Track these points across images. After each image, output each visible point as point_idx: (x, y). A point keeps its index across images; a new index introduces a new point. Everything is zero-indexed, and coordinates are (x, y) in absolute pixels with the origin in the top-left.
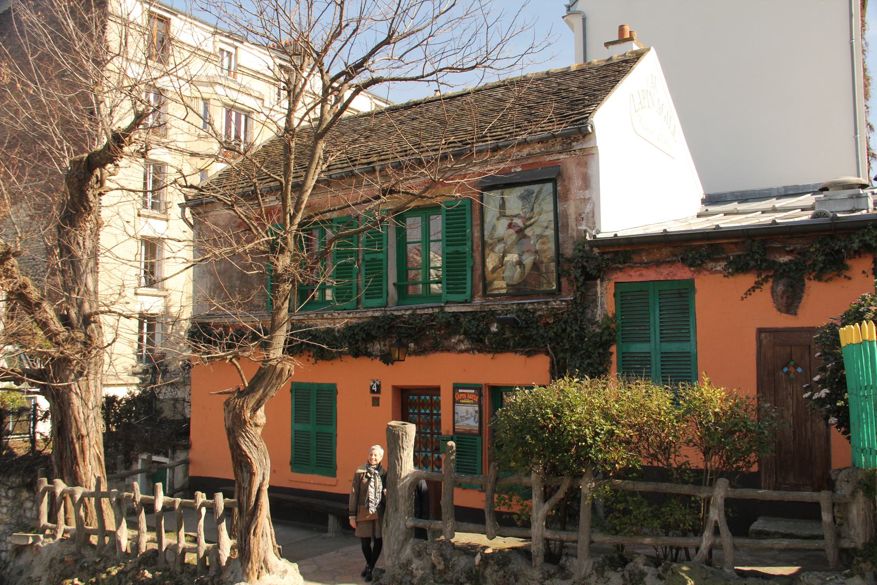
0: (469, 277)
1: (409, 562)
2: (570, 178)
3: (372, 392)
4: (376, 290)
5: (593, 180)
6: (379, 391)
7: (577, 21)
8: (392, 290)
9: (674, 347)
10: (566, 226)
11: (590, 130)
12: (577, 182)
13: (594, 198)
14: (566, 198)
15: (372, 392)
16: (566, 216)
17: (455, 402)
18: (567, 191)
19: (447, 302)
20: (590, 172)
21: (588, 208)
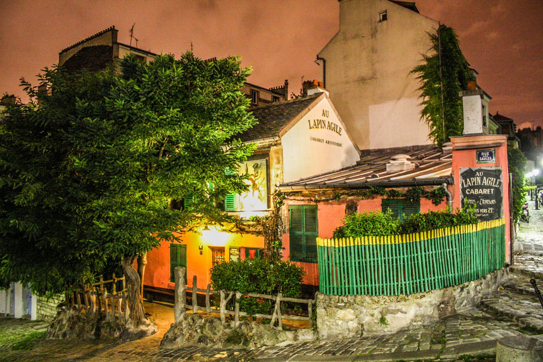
1: (182, 321)
3: (200, 249)
7: (321, 63)
9: (309, 233)
15: (200, 249)
17: (230, 254)
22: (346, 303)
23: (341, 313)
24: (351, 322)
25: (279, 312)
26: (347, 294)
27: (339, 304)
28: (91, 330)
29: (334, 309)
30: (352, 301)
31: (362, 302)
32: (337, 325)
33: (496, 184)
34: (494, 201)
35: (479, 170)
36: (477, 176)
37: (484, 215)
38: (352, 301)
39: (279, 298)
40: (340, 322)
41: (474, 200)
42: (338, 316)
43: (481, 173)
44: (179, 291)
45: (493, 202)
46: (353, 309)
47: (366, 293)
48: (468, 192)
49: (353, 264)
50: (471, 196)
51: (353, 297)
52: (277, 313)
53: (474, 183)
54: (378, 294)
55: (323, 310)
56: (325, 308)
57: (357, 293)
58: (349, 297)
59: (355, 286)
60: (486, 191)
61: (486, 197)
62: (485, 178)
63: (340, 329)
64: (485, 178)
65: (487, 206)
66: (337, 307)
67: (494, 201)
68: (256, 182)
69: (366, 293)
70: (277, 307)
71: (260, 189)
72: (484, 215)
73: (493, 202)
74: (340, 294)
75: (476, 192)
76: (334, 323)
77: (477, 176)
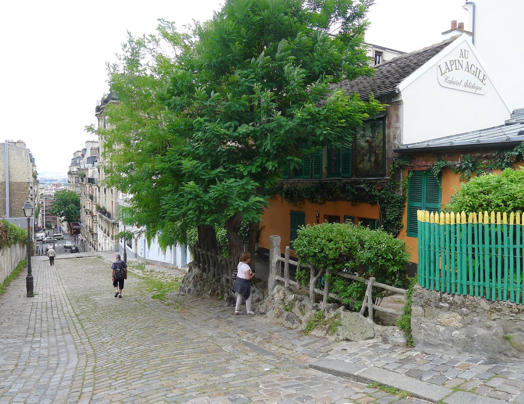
0: (351, 165)
2: (391, 117)
4: (318, 170)
5: (401, 118)
6: (319, 217)
8: (324, 170)
10: (389, 141)
11: (397, 92)
12: (394, 119)
13: (401, 127)
14: (389, 127)
16: (389, 136)
18: (390, 123)
19: (343, 177)
20: (399, 113)
21: (398, 132)
22: (451, 304)
23: (445, 317)
24: (457, 332)
25: (370, 300)
26: (453, 292)
27: (441, 304)
28: (209, 290)
29: (434, 309)
30: (459, 302)
31: (475, 307)
32: (438, 332)
38: (459, 302)
39: (370, 282)
40: (442, 329)
42: (439, 320)
44: (273, 261)
46: (461, 315)
47: (482, 294)
49: (464, 251)
51: (462, 297)
52: (367, 302)
54: (500, 298)
55: (420, 308)
56: (422, 306)
57: (468, 292)
58: (456, 296)
59: (465, 282)
63: (441, 338)
66: (437, 307)
68: (373, 144)
69: (482, 294)
70: (368, 293)
71: (377, 152)
74: (443, 290)
76: (433, 328)
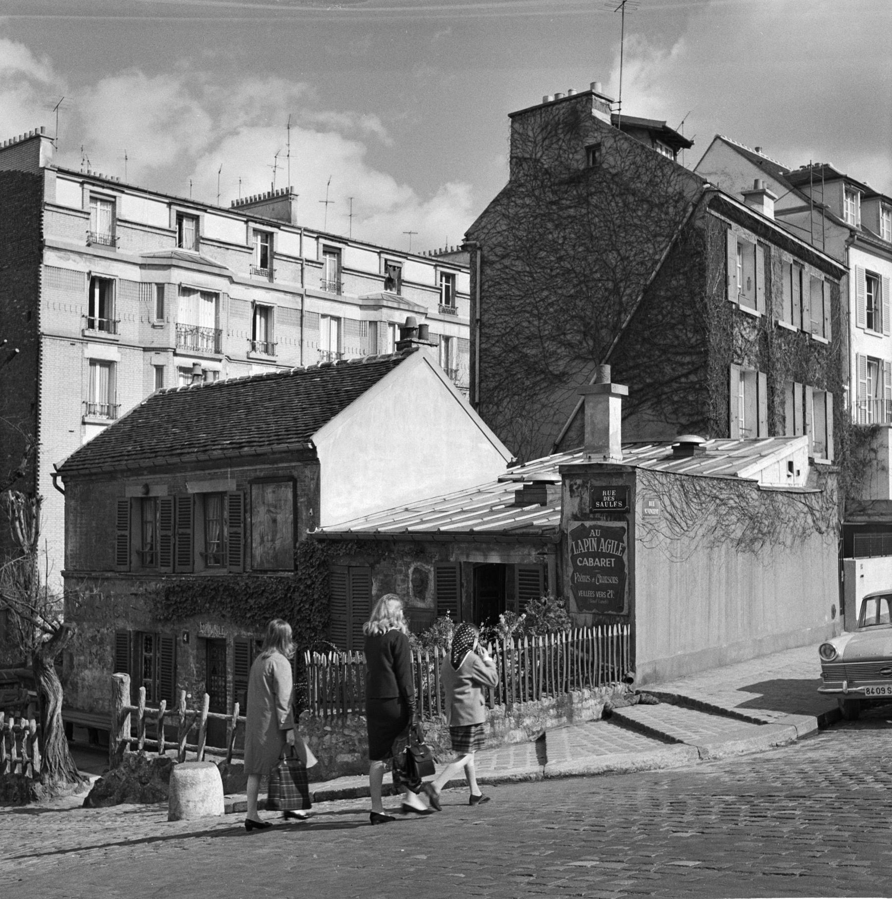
33: (617, 549)
34: (616, 578)
35: (594, 527)
36: (592, 537)
37: (602, 602)
41: (588, 577)
43: (598, 533)
45: (614, 580)
48: (581, 562)
50: (584, 570)
53: (588, 548)
60: (604, 562)
61: (605, 571)
62: (603, 540)
64: (603, 540)
65: (604, 588)
67: (616, 578)
72: (602, 602)
73: (614, 580)
75: (590, 562)
77: (592, 537)
